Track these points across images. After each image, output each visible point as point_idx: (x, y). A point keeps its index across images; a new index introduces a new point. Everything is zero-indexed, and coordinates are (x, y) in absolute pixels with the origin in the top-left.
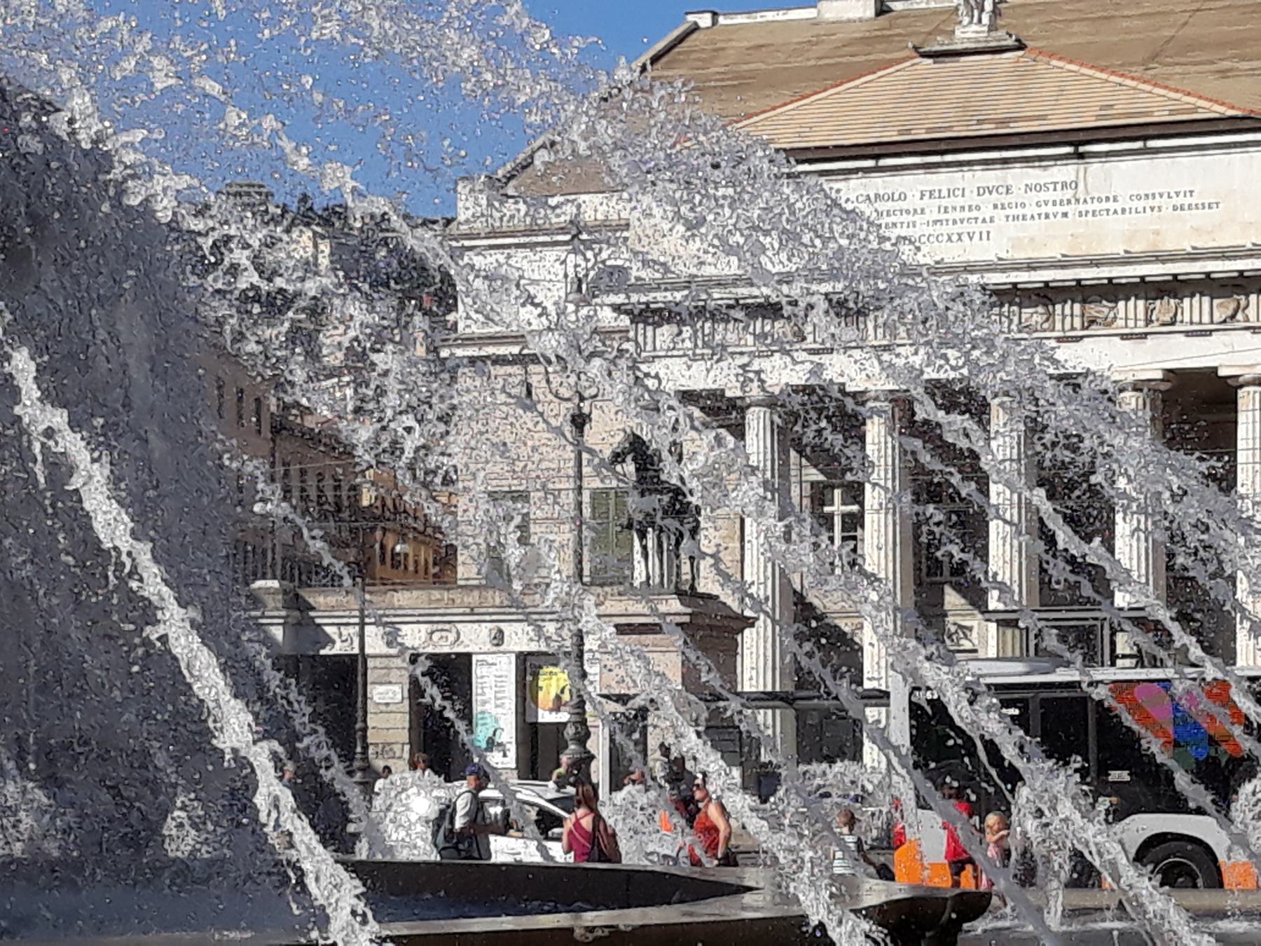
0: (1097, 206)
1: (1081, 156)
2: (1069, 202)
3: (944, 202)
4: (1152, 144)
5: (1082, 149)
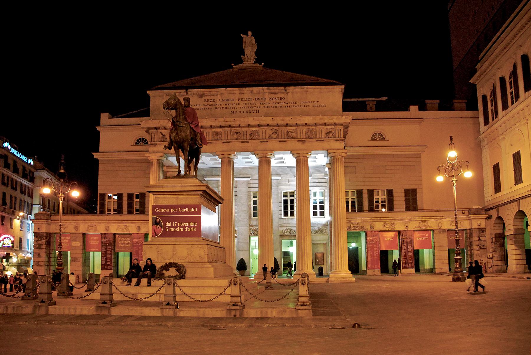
0: (291, 105)
1: (286, 90)
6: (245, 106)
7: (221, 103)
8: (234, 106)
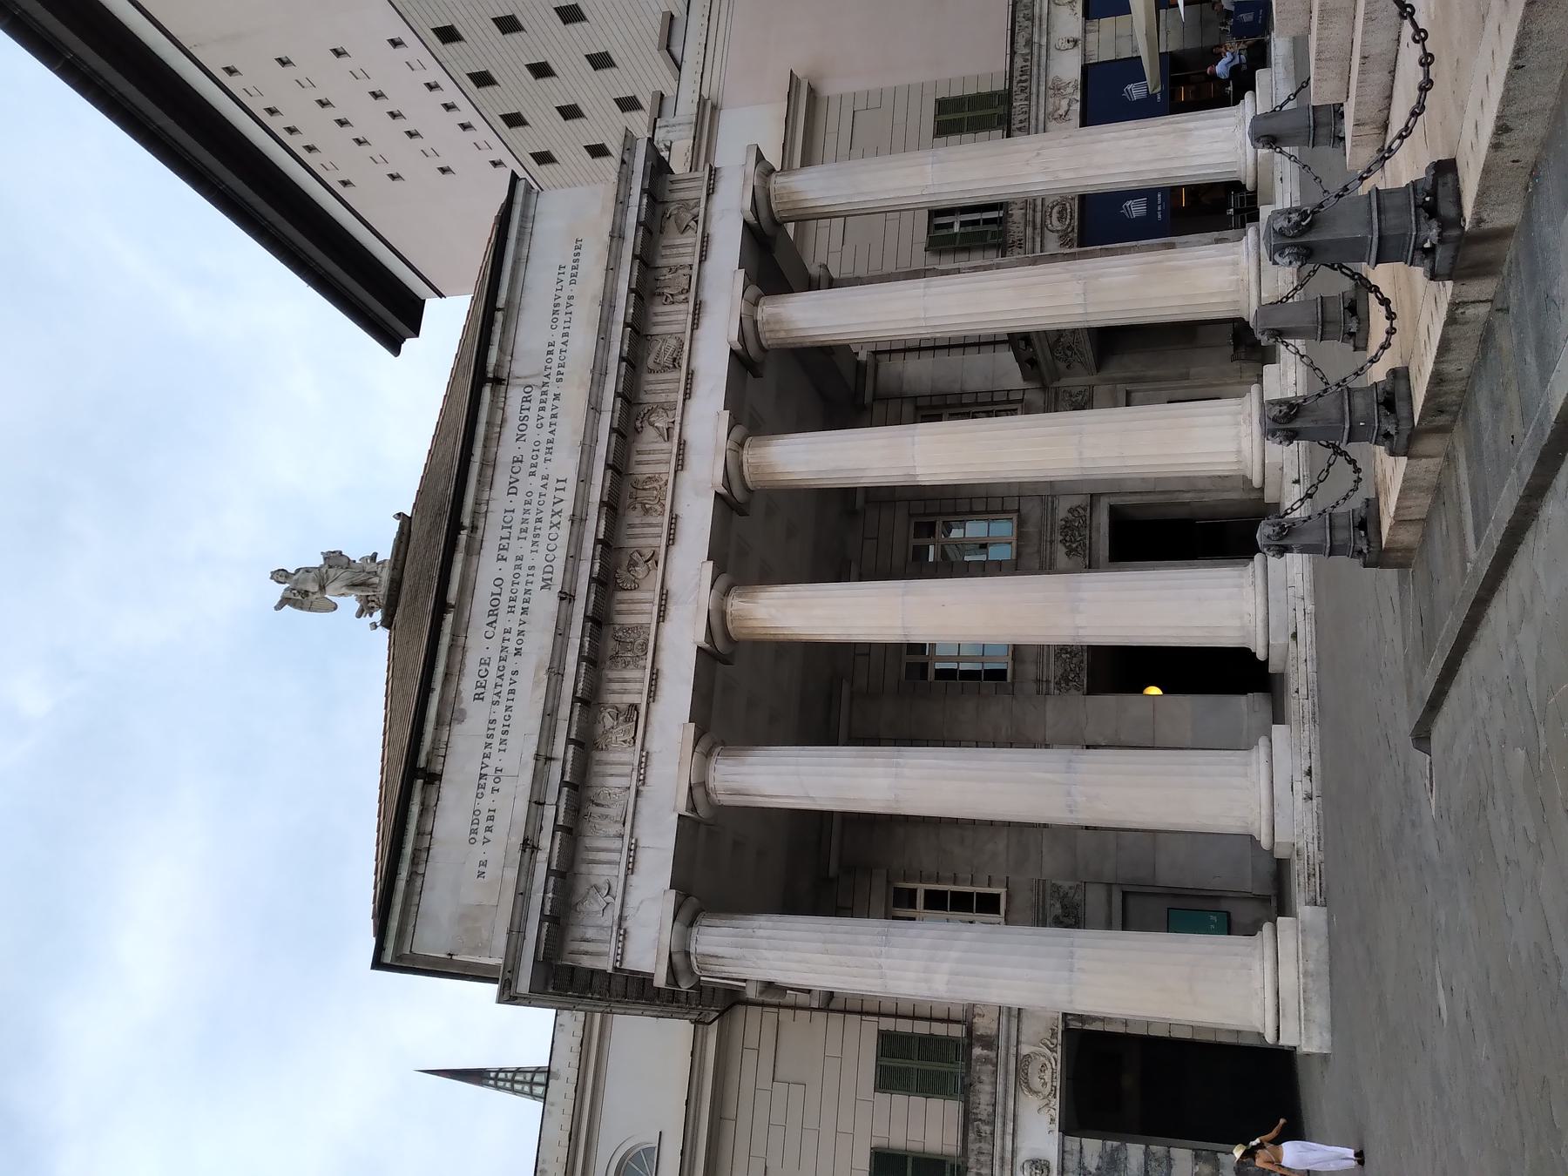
0: (555, 364)
1: (498, 381)
2: (545, 393)
3: (515, 532)
4: (501, 303)
5: (490, 375)
6: (531, 532)
8: (522, 580)
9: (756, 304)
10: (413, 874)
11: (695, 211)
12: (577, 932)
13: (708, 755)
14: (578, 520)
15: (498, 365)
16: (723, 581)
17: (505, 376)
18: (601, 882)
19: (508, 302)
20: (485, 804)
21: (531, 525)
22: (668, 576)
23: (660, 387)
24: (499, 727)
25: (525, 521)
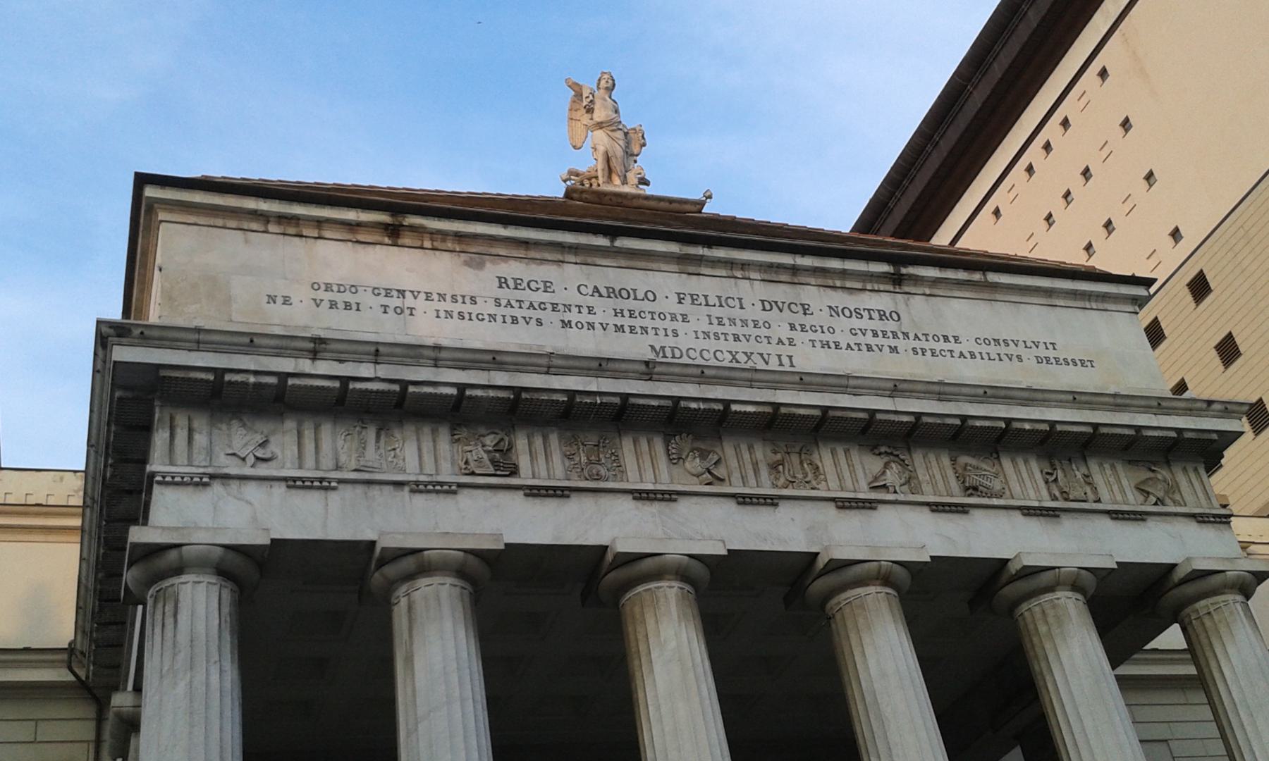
0: (932, 344)
1: (897, 280)
2: (895, 335)
3: (716, 312)
4: (993, 277)
5: (904, 271)
6: (720, 329)
7: (590, 301)
8: (658, 323)
9: (1076, 587)
10: (264, 217)
11: (1168, 501)
12: (200, 422)
13: (461, 572)
14: (752, 378)
15: (917, 280)
16: (698, 569)
17: (906, 289)
18: (274, 448)
19: (995, 287)
20: (366, 298)
21: (731, 330)
22: (695, 499)
23: (936, 472)
24: (468, 308)
25: (732, 322)
